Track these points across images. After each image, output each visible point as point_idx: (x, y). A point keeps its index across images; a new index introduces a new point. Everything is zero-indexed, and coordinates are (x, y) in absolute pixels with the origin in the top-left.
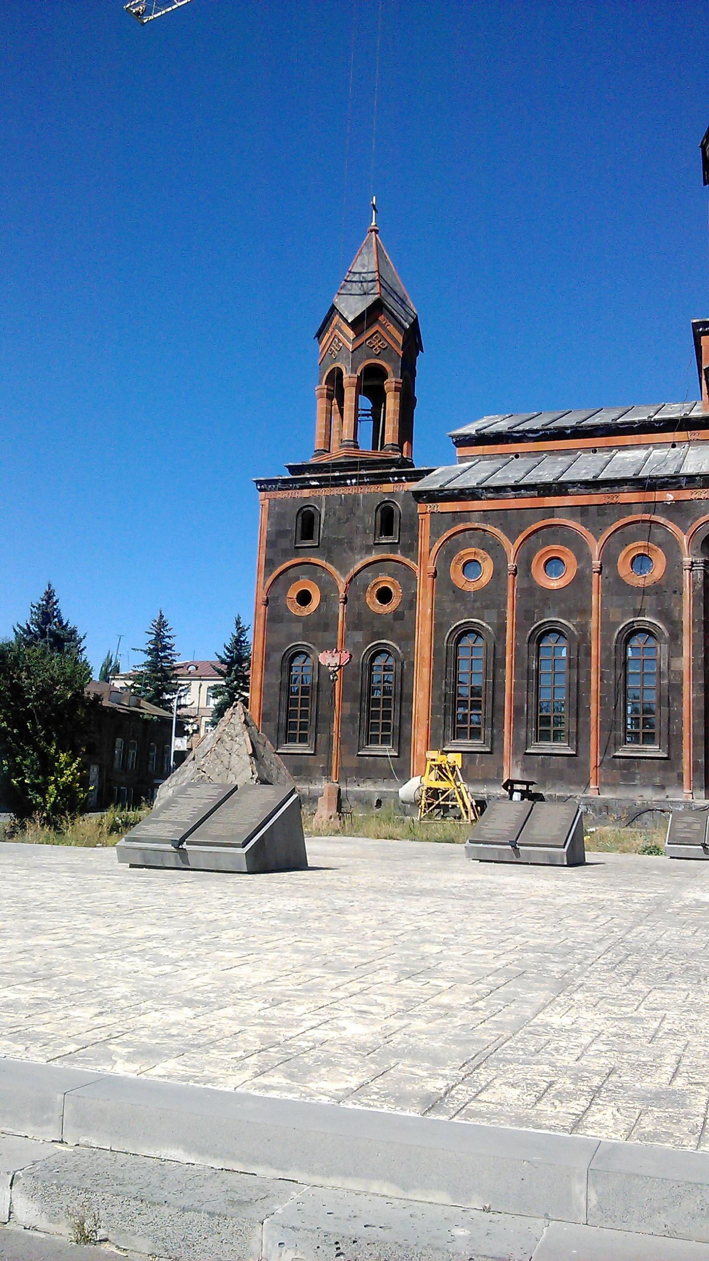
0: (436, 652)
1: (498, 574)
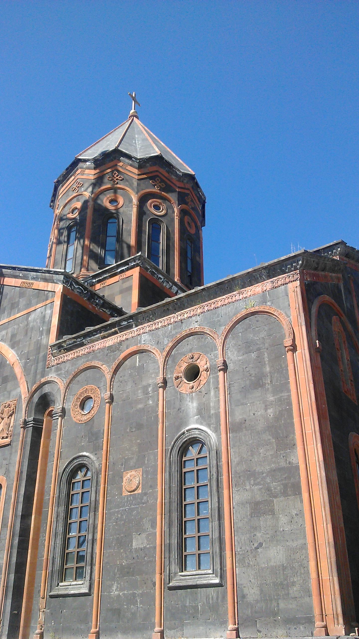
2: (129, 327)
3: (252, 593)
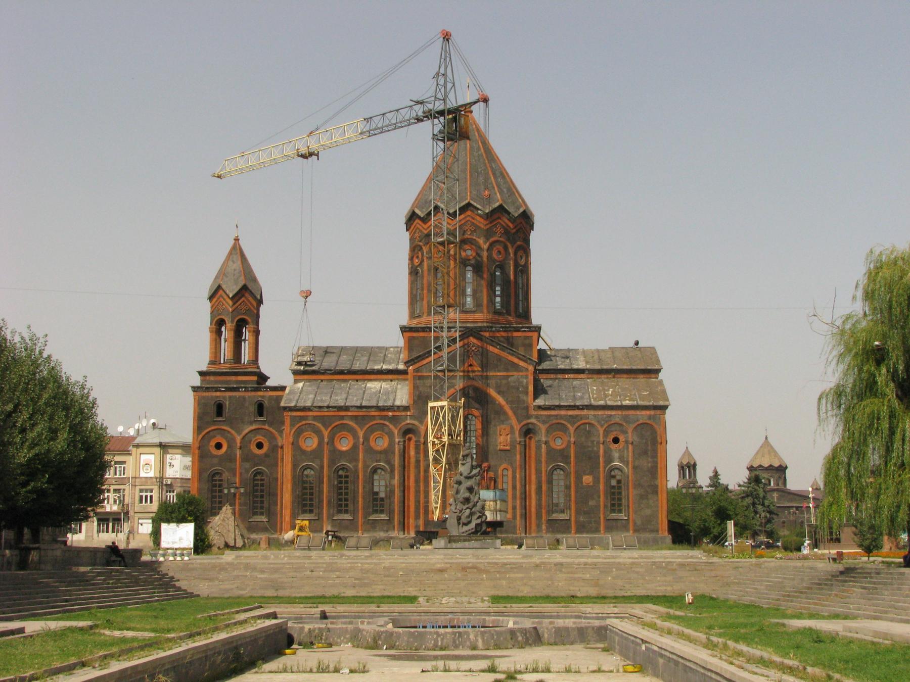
0: (294, 477)
1: (320, 444)
2: (583, 409)
3: (639, 523)
